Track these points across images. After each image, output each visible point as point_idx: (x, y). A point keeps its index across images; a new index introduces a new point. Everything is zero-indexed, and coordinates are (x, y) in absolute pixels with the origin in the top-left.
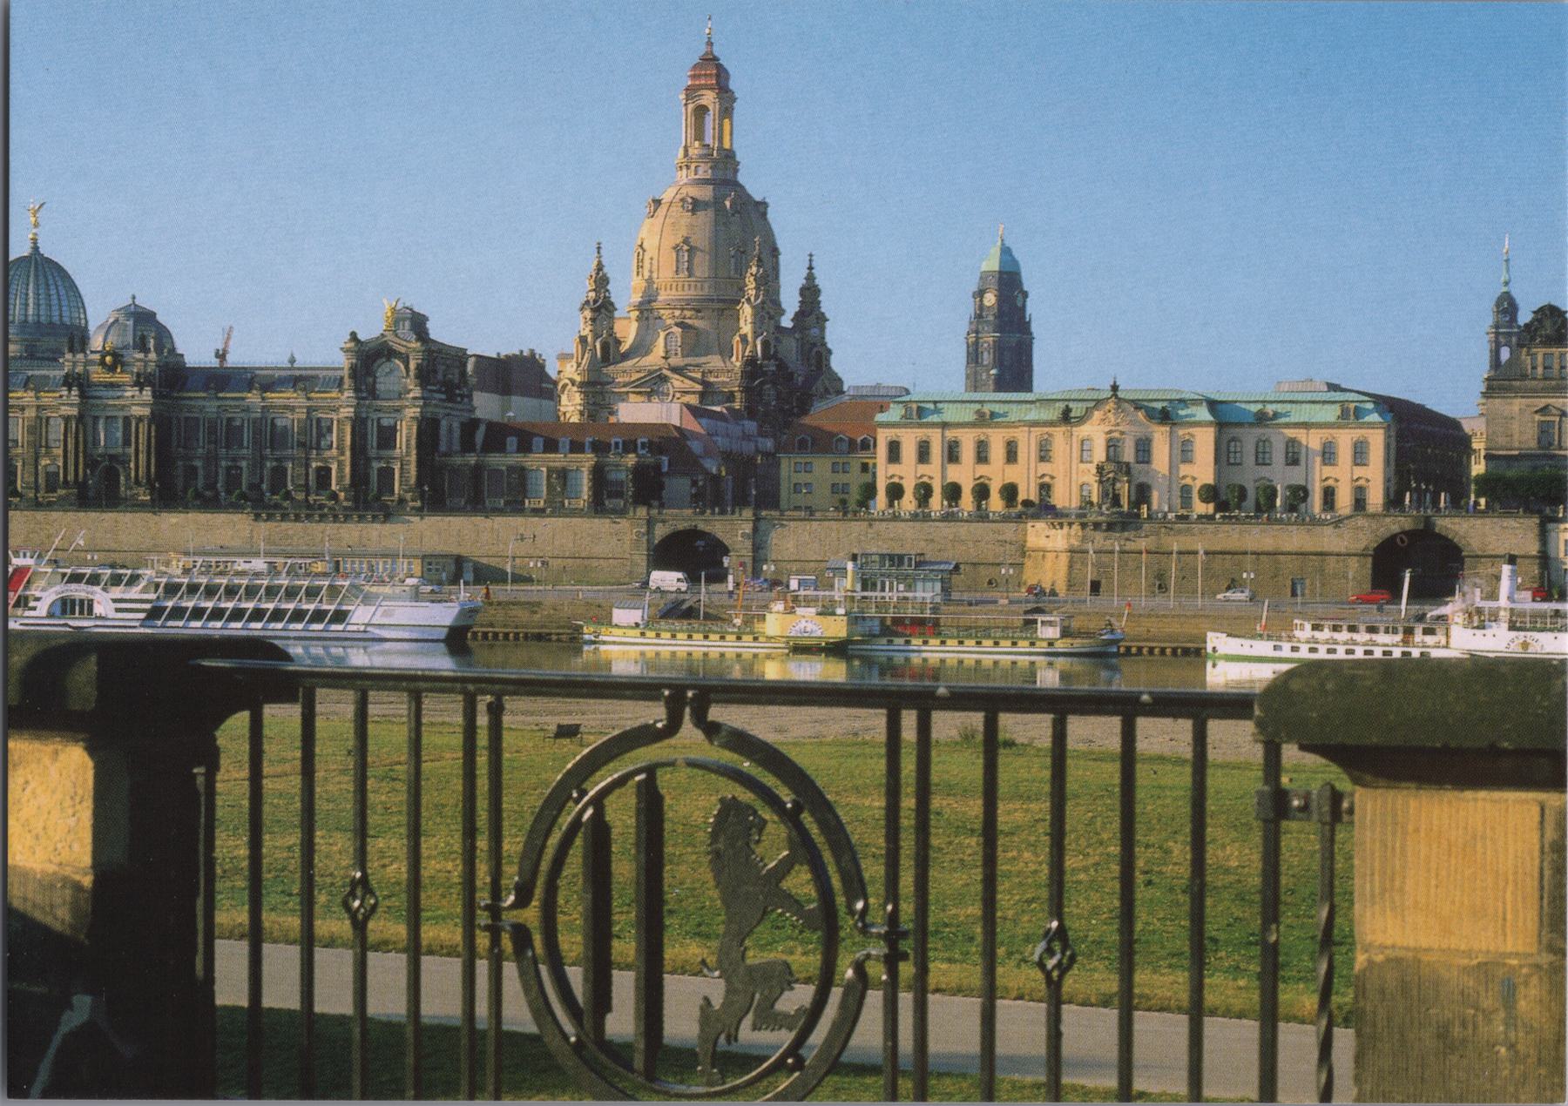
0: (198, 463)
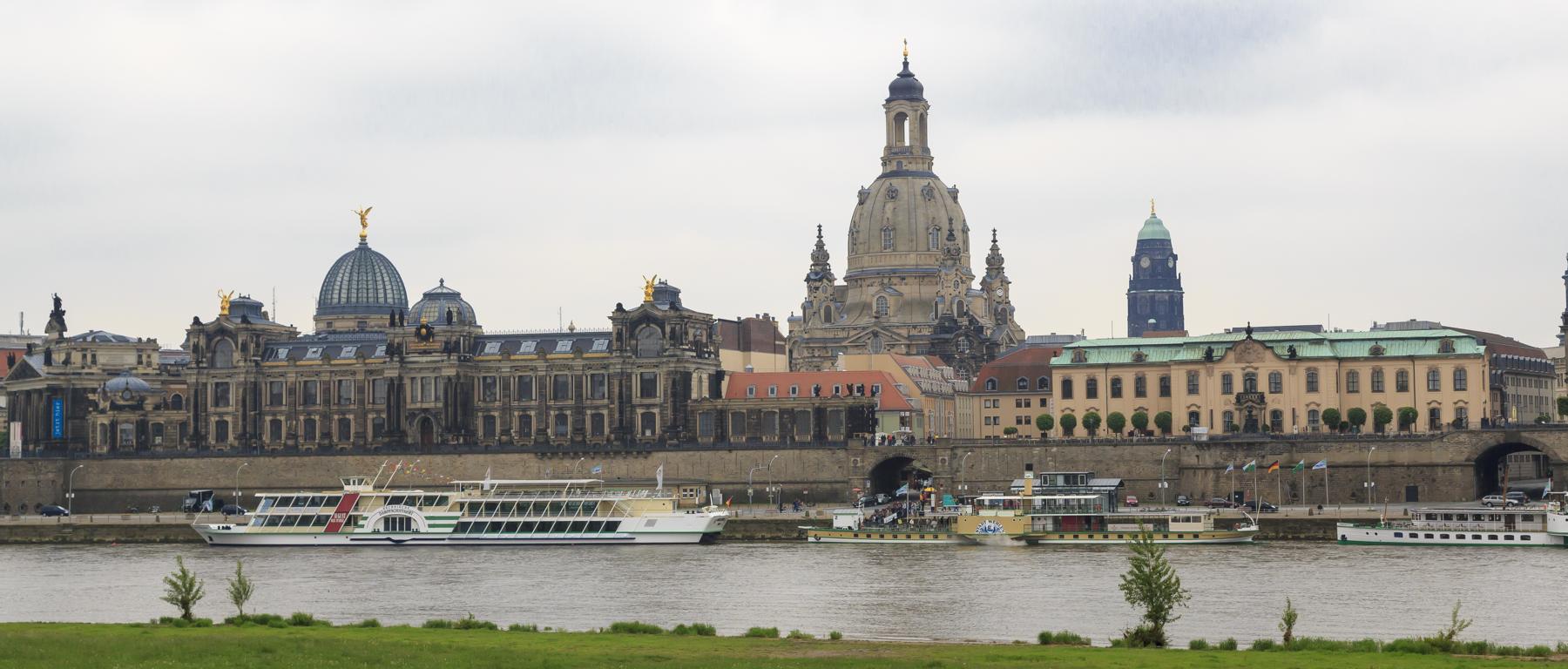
0: (496, 414)
